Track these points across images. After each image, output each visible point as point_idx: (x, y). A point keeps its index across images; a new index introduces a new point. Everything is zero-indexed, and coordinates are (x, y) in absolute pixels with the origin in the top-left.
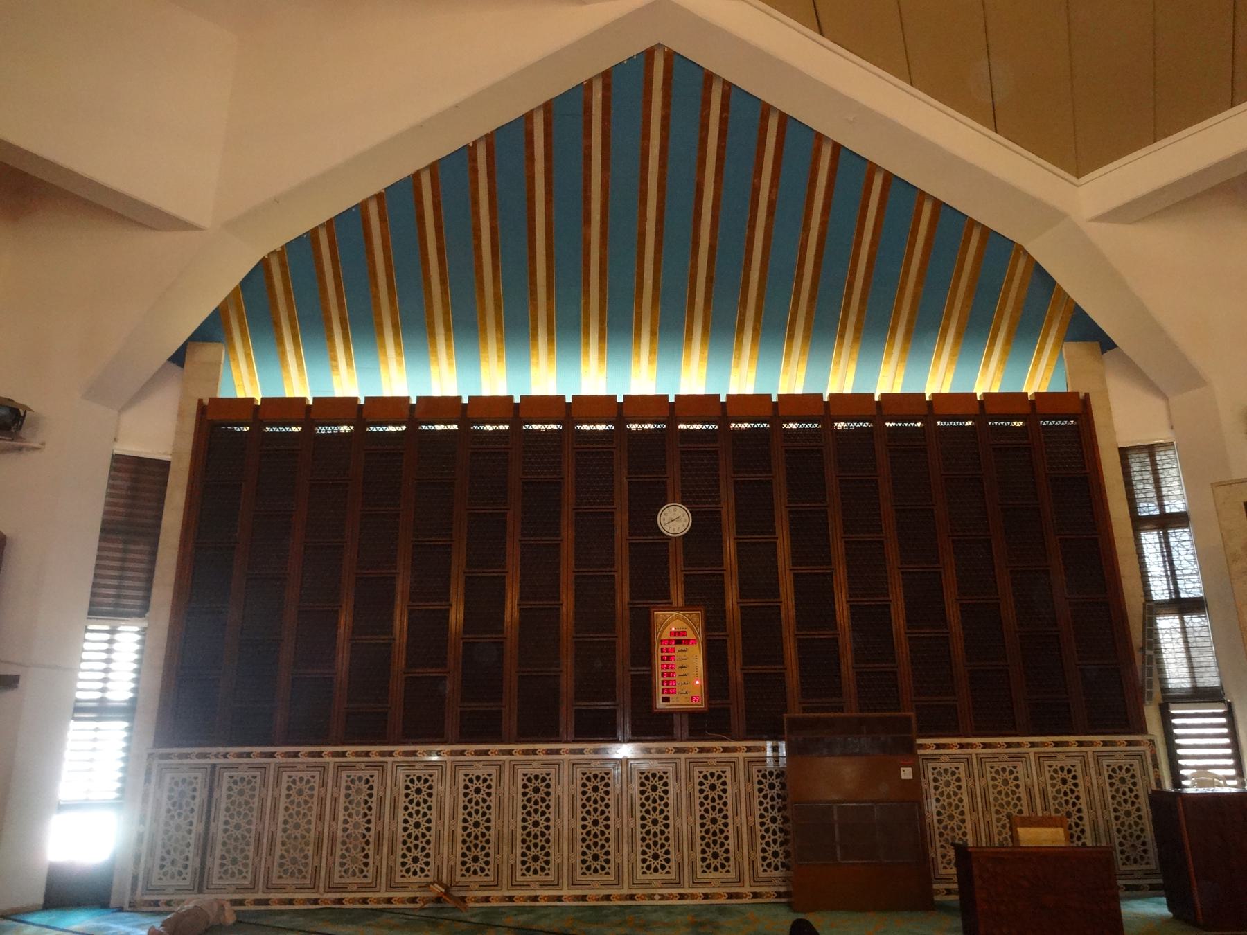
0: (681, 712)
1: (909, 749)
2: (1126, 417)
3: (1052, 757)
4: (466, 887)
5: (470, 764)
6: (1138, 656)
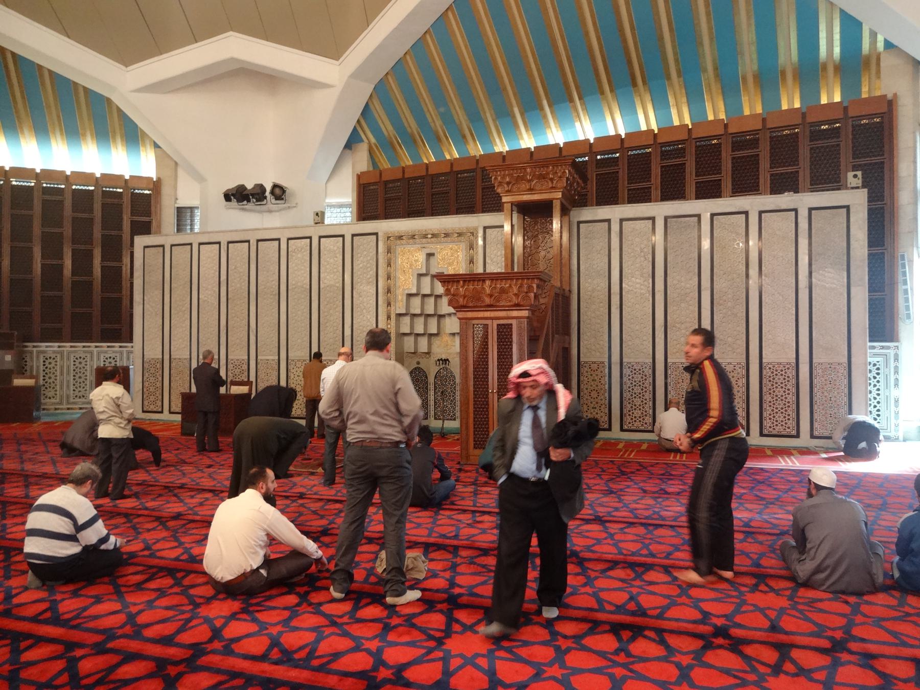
3: (106, 352)
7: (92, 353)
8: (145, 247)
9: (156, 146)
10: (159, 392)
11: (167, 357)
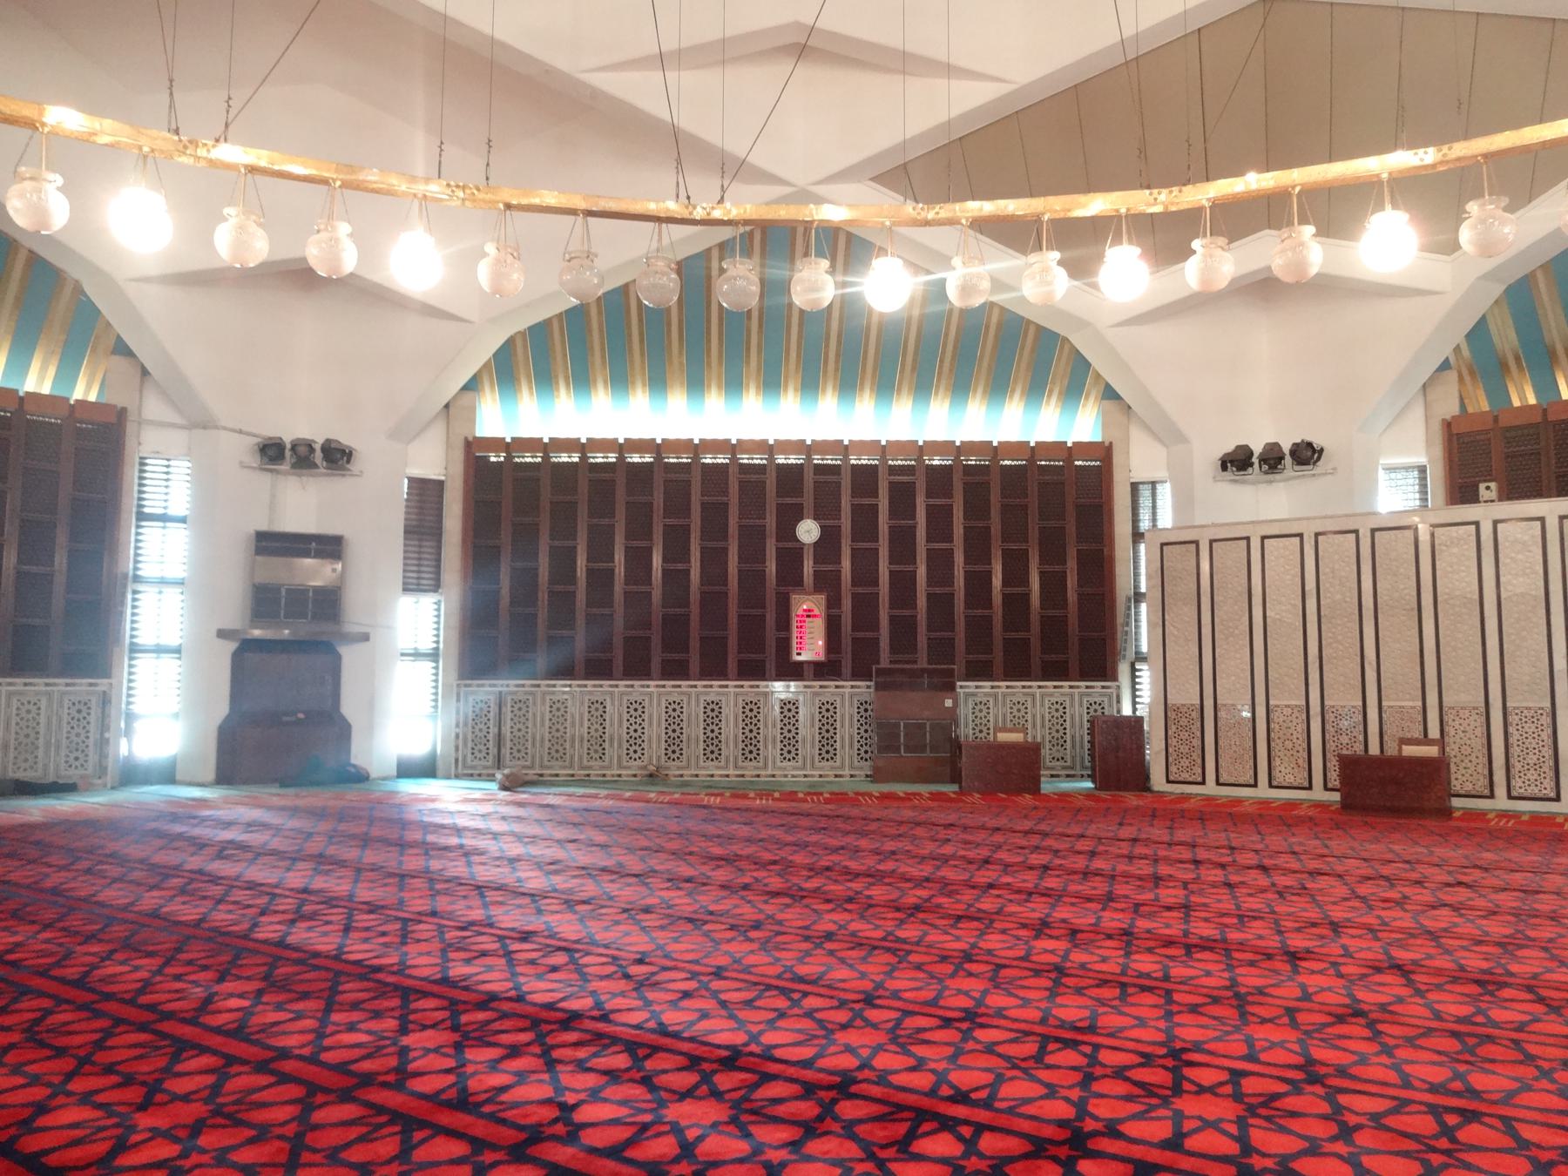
0: (809, 662)
1: (951, 688)
2: (1139, 459)
3: (1051, 695)
4: (668, 768)
5: (670, 693)
6: (1119, 628)
7: (1033, 696)
8: (1163, 545)
9: (1110, 394)
10: (1196, 755)
11: (1209, 703)
